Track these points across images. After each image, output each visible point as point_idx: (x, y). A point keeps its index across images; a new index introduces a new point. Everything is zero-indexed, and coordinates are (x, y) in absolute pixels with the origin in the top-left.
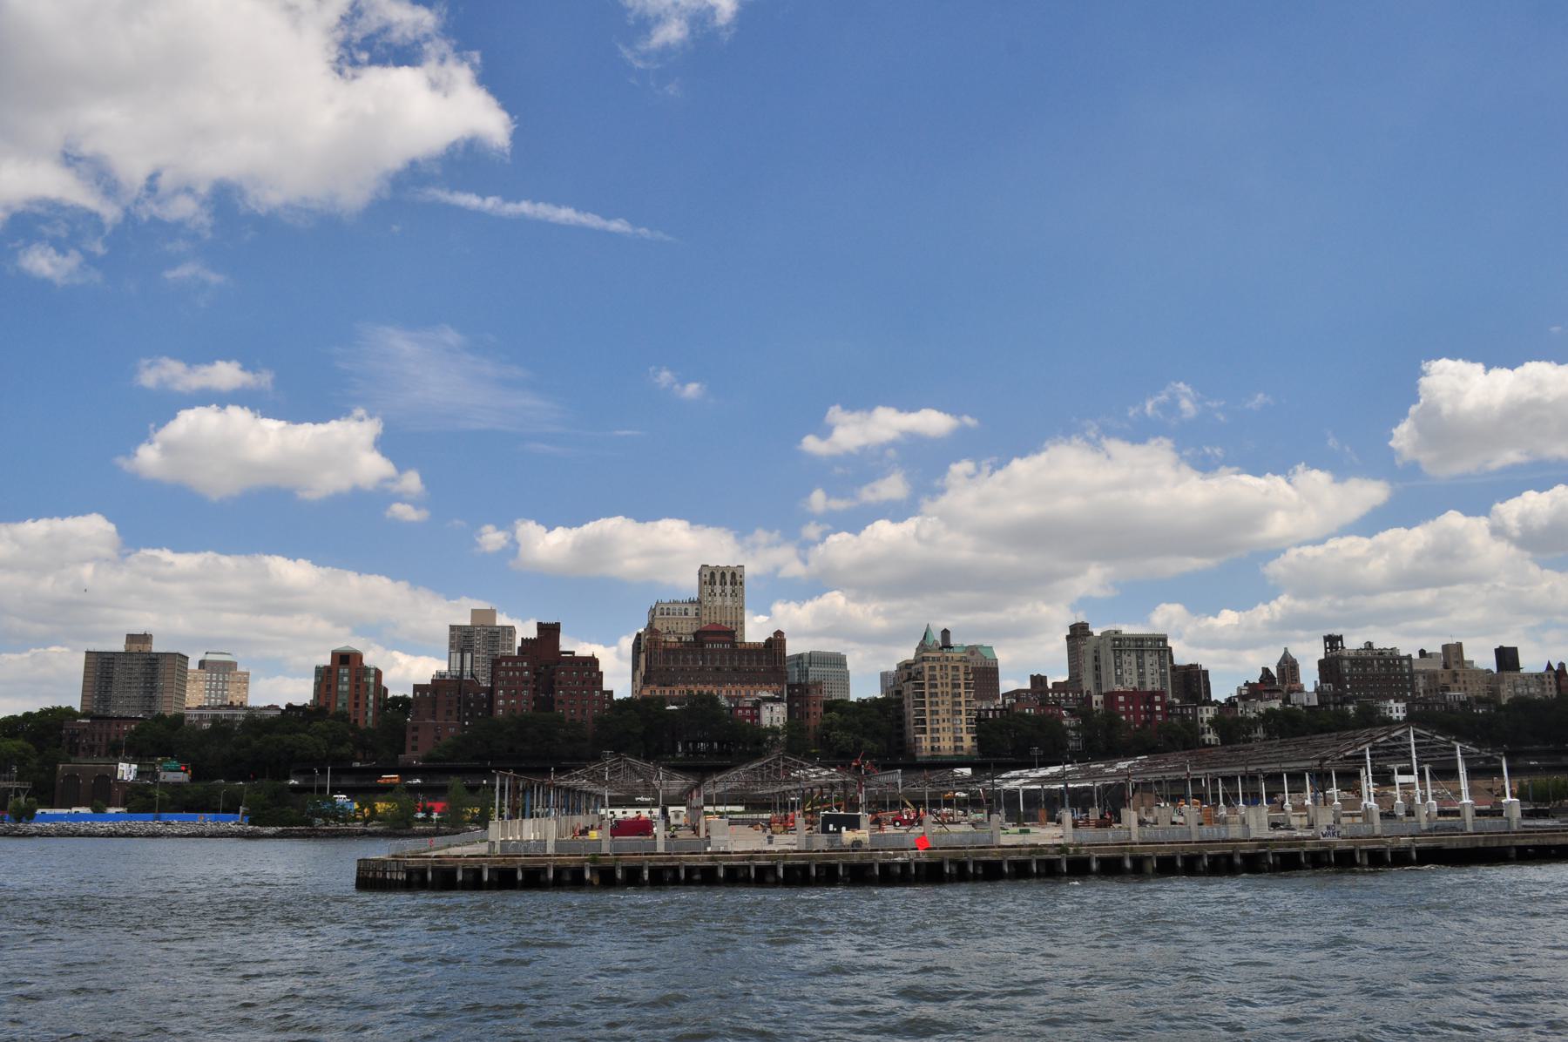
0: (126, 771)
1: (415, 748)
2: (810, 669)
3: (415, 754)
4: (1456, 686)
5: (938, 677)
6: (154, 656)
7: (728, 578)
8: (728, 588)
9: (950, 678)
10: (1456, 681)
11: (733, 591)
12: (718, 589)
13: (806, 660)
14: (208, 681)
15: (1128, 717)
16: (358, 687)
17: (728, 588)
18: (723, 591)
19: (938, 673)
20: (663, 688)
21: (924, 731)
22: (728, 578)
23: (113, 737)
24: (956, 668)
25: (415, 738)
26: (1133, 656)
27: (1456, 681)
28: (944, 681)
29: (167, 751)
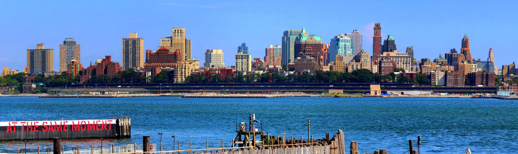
0: (34, 86)
1: (82, 81)
2: (290, 37)
3: (82, 82)
4: (335, 66)
5: (179, 67)
6: (44, 50)
7: (179, 31)
8: (179, 34)
9: (181, 67)
10: (335, 65)
11: (181, 35)
12: (177, 34)
13: (289, 33)
14: (67, 48)
15: (223, 75)
16: (76, 68)
17: (179, 34)
18: (178, 35)
19: (178, 66)
20: (149, 64)
21: (175, 77)
22: (179, 31)
23: (32, 79)
24: (182, 65)
25: (82, 79)
26: (241, 59)
27: (335, 65)
28: (180, 68)
29: (42, 82)
